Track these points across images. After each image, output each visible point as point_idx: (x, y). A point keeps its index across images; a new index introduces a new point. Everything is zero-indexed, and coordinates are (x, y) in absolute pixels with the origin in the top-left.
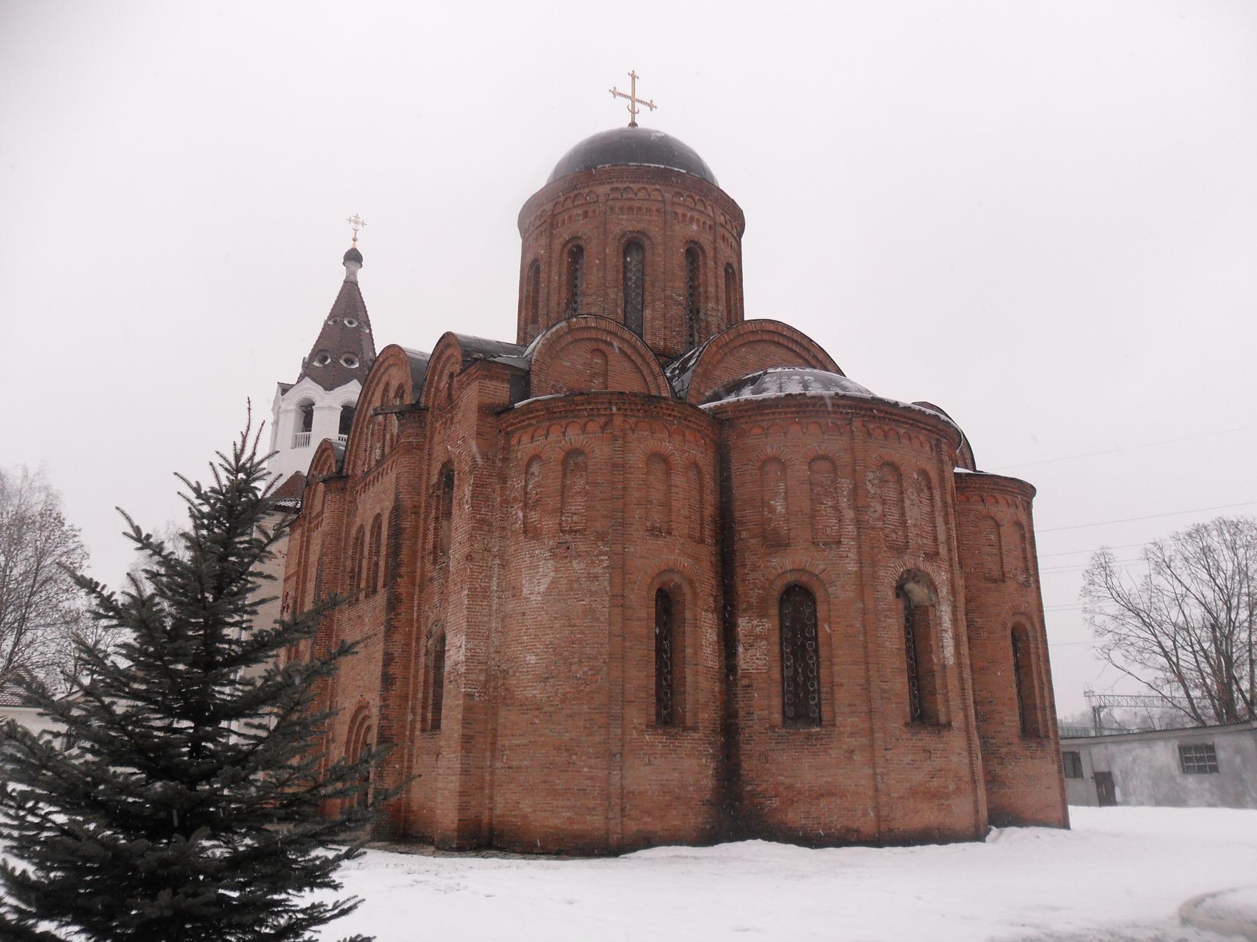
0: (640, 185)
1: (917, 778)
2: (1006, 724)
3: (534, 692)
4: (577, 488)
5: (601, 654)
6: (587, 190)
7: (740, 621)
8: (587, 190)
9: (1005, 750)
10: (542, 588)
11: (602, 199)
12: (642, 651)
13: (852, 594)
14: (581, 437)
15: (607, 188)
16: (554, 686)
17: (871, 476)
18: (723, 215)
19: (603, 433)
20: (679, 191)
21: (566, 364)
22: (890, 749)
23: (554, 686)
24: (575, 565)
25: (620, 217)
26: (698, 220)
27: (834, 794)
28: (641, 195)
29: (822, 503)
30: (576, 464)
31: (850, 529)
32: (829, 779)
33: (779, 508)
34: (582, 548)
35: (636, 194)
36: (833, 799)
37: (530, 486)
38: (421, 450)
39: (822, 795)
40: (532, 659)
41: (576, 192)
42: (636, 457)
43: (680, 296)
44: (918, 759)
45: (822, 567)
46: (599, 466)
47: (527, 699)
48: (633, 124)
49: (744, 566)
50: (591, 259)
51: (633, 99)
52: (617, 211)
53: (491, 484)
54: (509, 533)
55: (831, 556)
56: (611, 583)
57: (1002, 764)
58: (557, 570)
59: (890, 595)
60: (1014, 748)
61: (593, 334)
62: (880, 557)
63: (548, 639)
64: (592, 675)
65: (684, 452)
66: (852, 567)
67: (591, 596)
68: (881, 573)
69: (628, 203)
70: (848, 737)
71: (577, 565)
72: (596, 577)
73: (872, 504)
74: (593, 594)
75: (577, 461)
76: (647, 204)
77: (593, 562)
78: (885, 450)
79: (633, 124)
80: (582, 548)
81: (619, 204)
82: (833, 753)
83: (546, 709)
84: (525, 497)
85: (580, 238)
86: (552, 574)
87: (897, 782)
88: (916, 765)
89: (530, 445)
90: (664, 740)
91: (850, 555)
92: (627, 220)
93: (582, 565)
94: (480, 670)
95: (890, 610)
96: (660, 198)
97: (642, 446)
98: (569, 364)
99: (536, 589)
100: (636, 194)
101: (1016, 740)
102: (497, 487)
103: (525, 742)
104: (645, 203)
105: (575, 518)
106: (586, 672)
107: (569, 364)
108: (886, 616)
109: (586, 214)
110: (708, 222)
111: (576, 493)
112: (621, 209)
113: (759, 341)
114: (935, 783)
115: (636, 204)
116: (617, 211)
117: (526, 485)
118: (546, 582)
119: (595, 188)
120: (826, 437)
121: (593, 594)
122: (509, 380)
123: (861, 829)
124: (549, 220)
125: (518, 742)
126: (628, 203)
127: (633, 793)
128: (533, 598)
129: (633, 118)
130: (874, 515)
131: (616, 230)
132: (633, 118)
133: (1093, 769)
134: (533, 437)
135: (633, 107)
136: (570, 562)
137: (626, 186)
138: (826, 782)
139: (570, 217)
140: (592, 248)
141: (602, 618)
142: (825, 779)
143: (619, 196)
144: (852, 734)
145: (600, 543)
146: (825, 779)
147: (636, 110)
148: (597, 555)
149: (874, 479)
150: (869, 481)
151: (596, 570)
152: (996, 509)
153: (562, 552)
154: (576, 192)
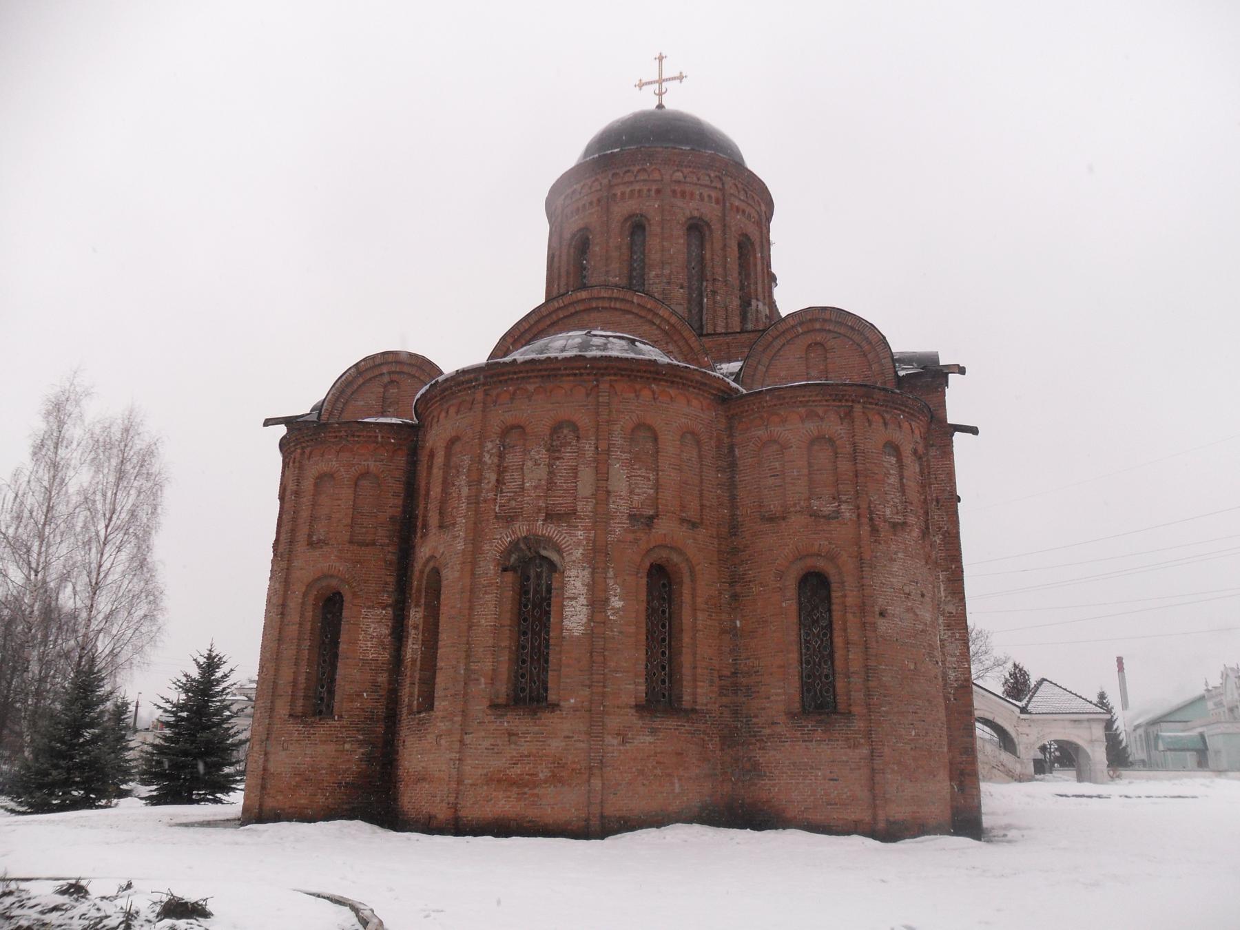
7: (412, 613)
9: (767, 731)
13: (457, 574)
17: (489, 445)
18: (678, 170)
22: (472, 733)
26: (640, 191)
36: (424, 784)
43: (616, 276)
44: (500, 743)
48: (660, 106)
51: (660, 81)
57: (763, 749)
60: (779, 729)
66: (460, 546)
68: (486, 547)
73: (487, 476)
78: (510, 413)
79: (660, 106)
87: (472, 767)
88: (496, 750)
90: (300, 729)
108: (486, 593)
110: (654, 187)
113: (572, 315)
114: (518, 770)
123: (438, 815)
129: (660, 100)
130: (486, 487)
132: (660, 100)
135: (660, 88)
138: (423, 768)
147: (664, 90)
149: (492, 449)
150: (488, 452)
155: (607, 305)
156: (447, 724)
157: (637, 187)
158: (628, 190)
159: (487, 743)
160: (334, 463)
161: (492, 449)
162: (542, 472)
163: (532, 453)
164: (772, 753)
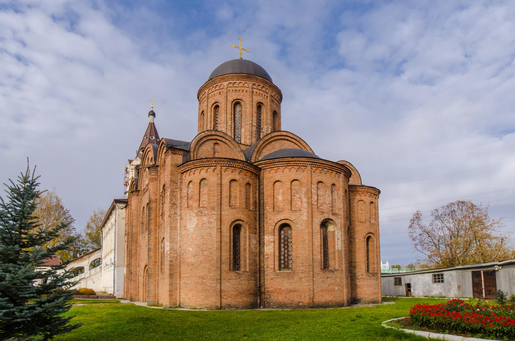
0: (240, 81)
1: (325, 286)
2: (362, 269)
3: (192, 260)
4: (205, 192)
5: (213, 248)
6: (220, 84)
8: (220, 84)
10: (193, 226)
11: (226, 87)
12: (227, 247)
13: (304, 227)
14: (206, 174)
15: (228, 82)
16: (198, 258)
19: (213, 173)
20: (255, 83)
21: (204, 148)
23: (198, 258)
24: (204, 218)
25: (232, 94)
26: (262, 94)
27: (295, 291)
28: (241, 85)
29: (295, 196)
30: (204, 184)
31: (305, 205)
32: (294, 287)
33: (280, 198)
34: (206, 212)
35: (238, 85)
36: (294, 293)
37: (189, 192)
38: (157, 180)
39: (291, 292)
40: (191, 249)
41: (216, 85)
42: (226, 181)
45: (294, 218)
46: (212, 184)
47: (189, 262)
49: (267, 218)
50: (222, 109)
52: (231, 91)
53: (176, 191)
54: (183, 208)
55: (297, 215)
56: (217, 225)
58: (198, 220)
59: (318, 227)
60: (364, 276)
61: (214, 137)
62: (315, 214)
63: (195, 243)
64: (210, 254)
65: (244, 179)
66: (305, 218)
67: (210, 229)
69: (235, 88)
70: (301, 274)
71: (205, 218)
72: (211, 222)
74: (210, 228)
75: (204, 183)
76: (243, 88)
77: (210, 217)
78: (320, 177)
80: (206, 212)
81: (232, 89)
82: (295, 279)
83: (195, 265)
84: (188, 195)
85: (218, 102)
86: (197, 222)
89: (189, 177)
91: (304, 214)
92: (235, 95)
93: (206, 219)
94: (175, 253)
95: (317, 232)
96: (247, 86)
97: (228, 177)
98: (205, 148)
99: (192, 227)
100: (238, 85)
101: (365, 274)
102: (179, 192)
103: (189, 275)
104: (241, 88)
105: (204, 203)
106: (208, 254)
107: (205, 148)
109: (220, 93)
111: (204, 194)
112: (233, 91)
115: (238, 89)
116: (231, 91)
117: (188, 192)
118: (195, 224)
119: (223, 83)
120: (297, 173)
121: (210, 228)
122: (182, 155)
124: (207, 96)
125: (187, 276)
126: (235, 88)
127: (224, 291)
128: (191, 229)
131: (230, 99)
133: (405, 282)
134: (189, 175)
136: (203, 217)
137: (234, 81)
139: (214, 95)
140: (222, 106)
141: (213, 236)
142: (292, 287)
143: (232, 86)
144: (302, 273)
145: (212, 211)
146: (292, 287)
148: (212, 215)
149: (314, 188)
151: (212, 220)
152: (364, 198)
153: (200, 214)
154: (216, 85)
155: (291, 140)
156: (305, 274)
157: (261, 92)
158: (259, 92)
159: (321, 280)
160: (238, 176)
161: (314, 188)
162: (330, 199)
163: (327, 192)
164: (361, 282)
